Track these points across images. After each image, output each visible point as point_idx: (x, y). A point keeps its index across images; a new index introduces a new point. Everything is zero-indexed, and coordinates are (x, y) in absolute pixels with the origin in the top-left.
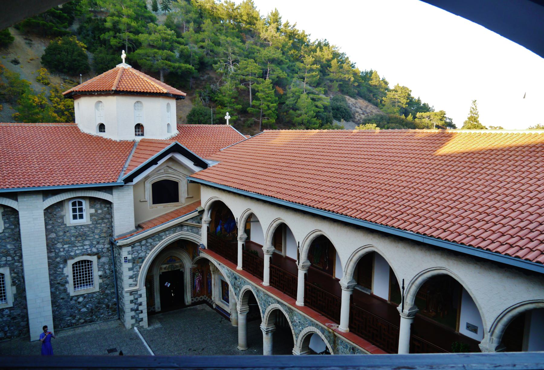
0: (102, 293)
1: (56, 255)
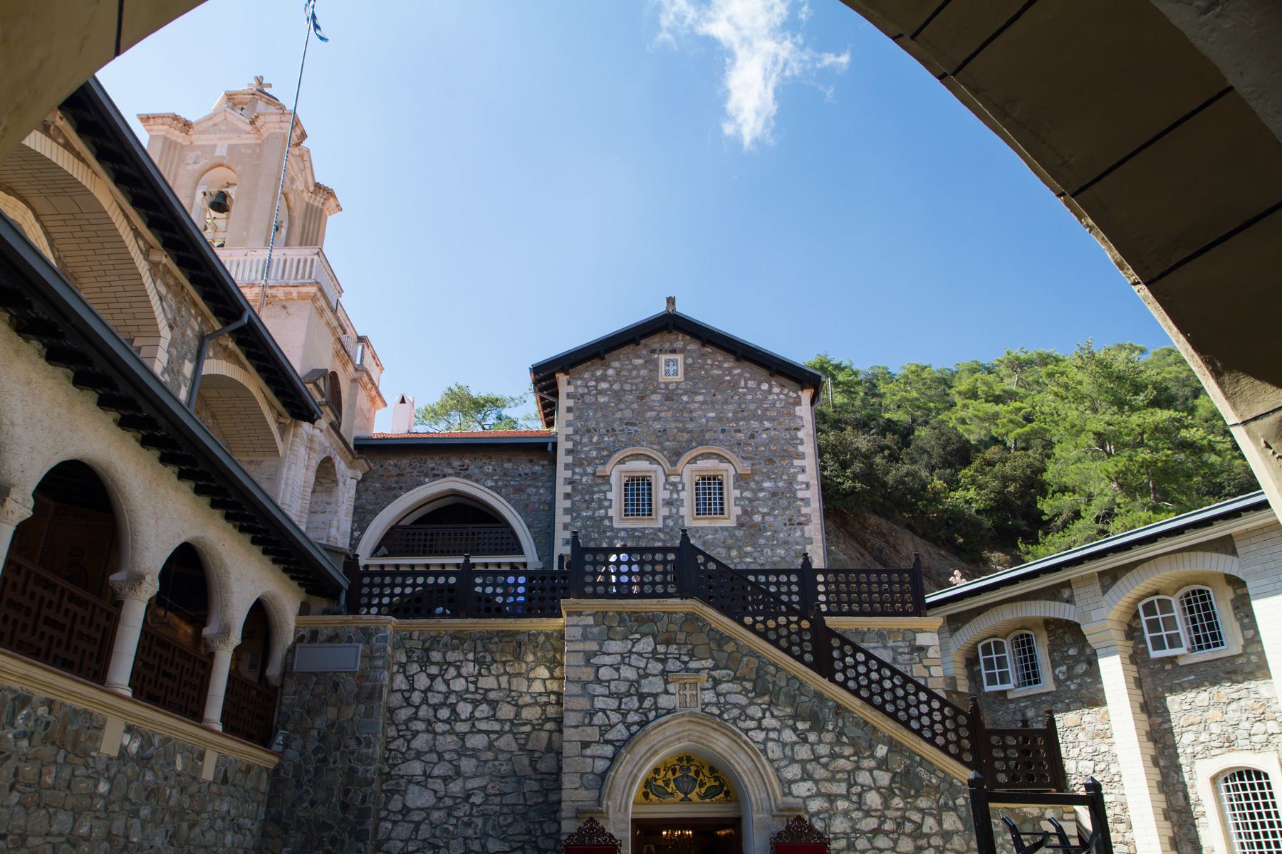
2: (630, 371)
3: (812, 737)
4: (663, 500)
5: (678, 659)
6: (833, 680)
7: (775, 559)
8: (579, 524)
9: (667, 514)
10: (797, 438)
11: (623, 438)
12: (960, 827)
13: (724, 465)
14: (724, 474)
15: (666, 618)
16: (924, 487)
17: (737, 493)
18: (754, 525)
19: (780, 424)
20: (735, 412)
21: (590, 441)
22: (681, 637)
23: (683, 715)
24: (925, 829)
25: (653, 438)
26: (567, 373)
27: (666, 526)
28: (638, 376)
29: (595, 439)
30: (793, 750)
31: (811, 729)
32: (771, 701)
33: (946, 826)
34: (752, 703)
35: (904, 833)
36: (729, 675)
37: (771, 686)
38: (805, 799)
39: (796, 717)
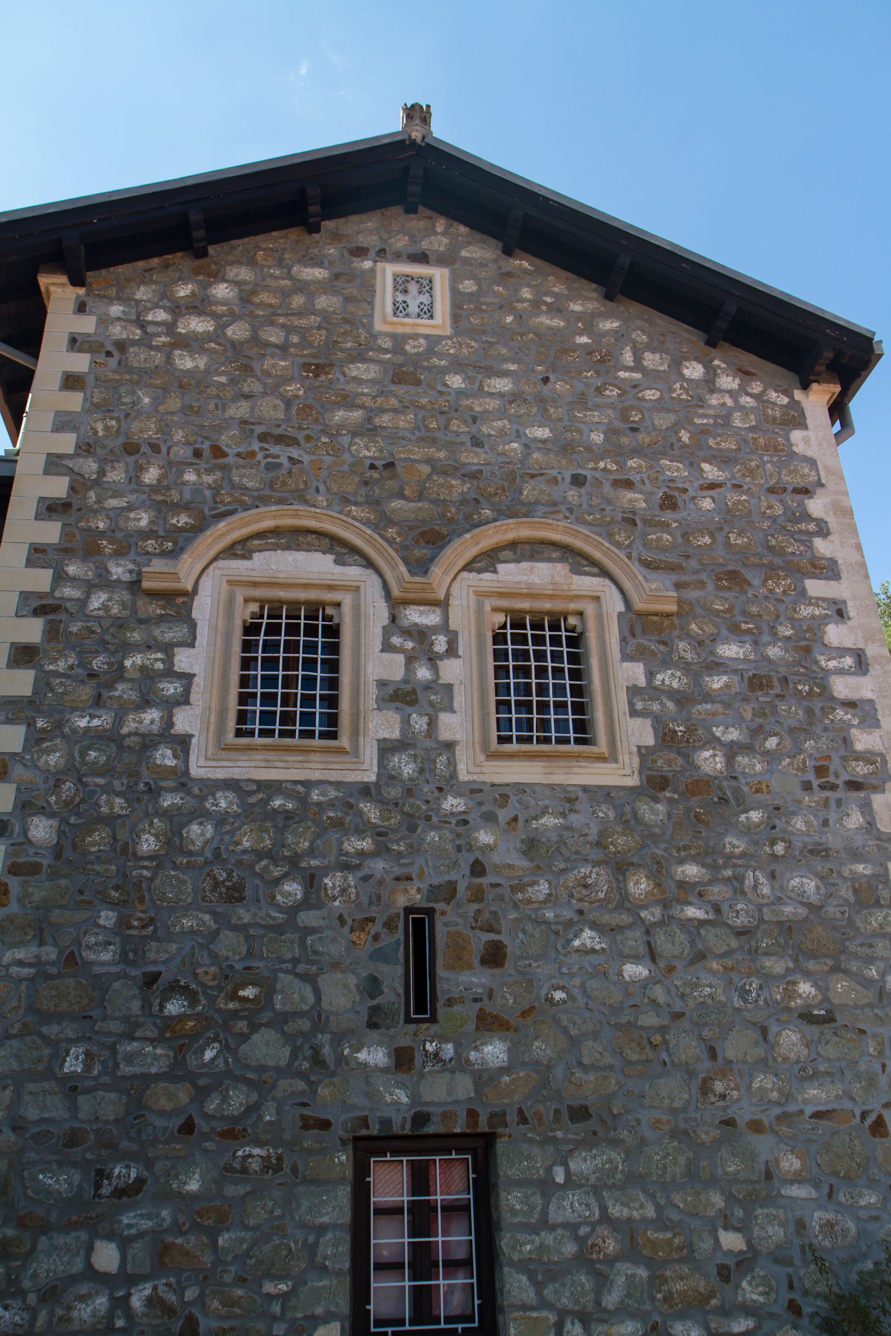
2: (286, 294)
4: (382, 684)
7: (788, 910)
8: (54, 759)
9: (396, 734)
10: (807, 517)
11: (250, 479)
14: (590, 610)
17: (635, 673)
19: (751, 472)
20: (611, 432)
21: (134, 479)
25: (350, 486)
26: (77, 281)
27: (387, 776)
28: (308, 310)
29: (151, 475)
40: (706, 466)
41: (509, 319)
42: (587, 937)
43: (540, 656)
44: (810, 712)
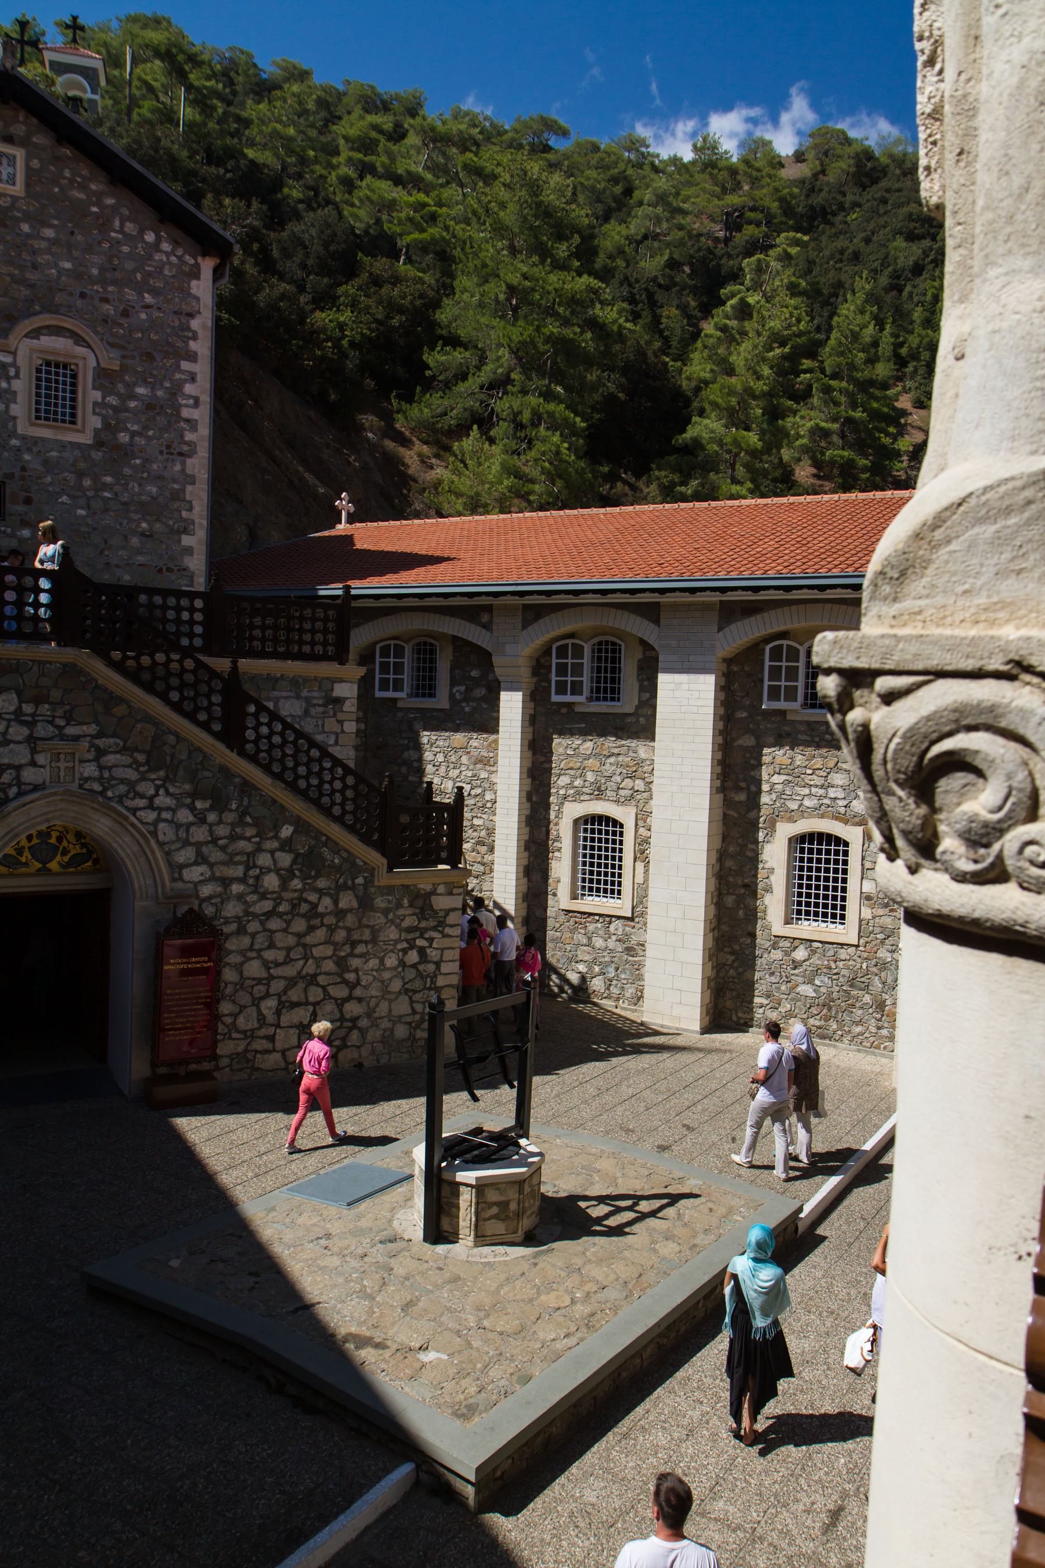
0: (865, 955)
1: (748, 798)
3: (212, 817)
5: (51, 723)
6: (242, 753)
10: (189, 329)
12: (355, 904)
13: (81, 350)
14: (81, 363)
15: (35, 668)
16: (302, 321)
17: (97, 395)
18: (118, 447)
20: (102, 269)
22: (56, 694)
23: (55, 794)
24: (321, 909)
30: (188, 831)
31: (212, 808)
32: (167, 776)
33: (342, 905)
34: (143, 778)
35: (298, 914)
36: (117, 745)
37: (168, 759)
38: (196, 884)
39: (195, 795)
40: (146, 295)
41: (56, 190)
42: (65, 499)
43: (57, 382)
44: (169, 422)
